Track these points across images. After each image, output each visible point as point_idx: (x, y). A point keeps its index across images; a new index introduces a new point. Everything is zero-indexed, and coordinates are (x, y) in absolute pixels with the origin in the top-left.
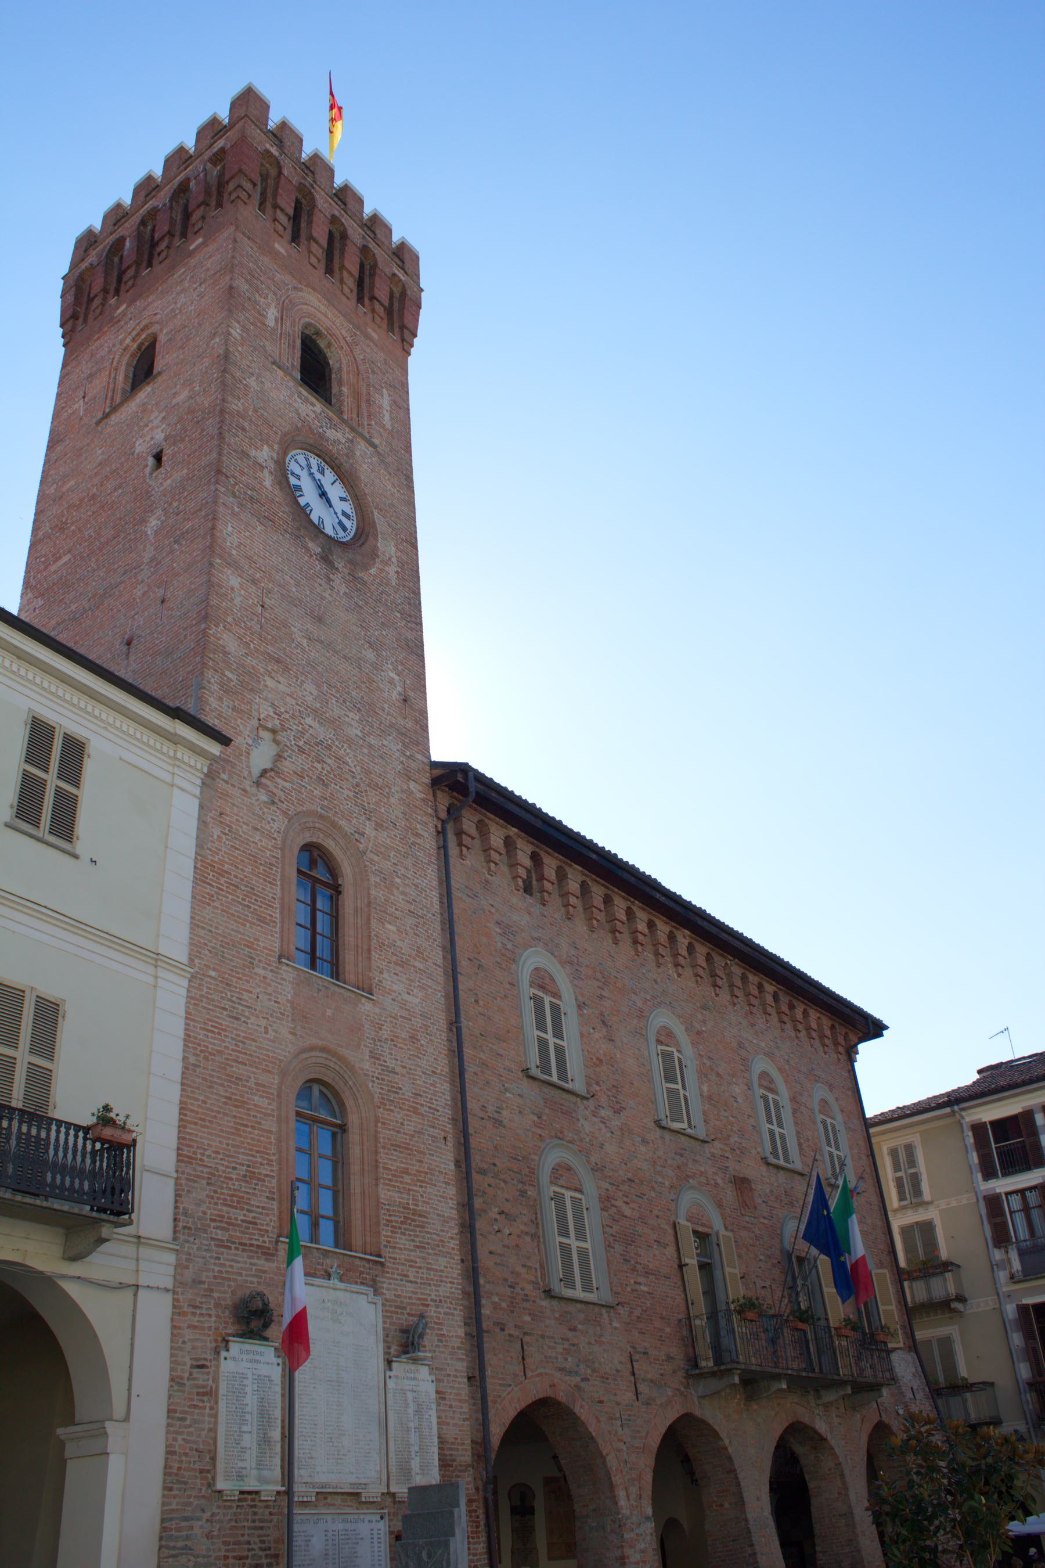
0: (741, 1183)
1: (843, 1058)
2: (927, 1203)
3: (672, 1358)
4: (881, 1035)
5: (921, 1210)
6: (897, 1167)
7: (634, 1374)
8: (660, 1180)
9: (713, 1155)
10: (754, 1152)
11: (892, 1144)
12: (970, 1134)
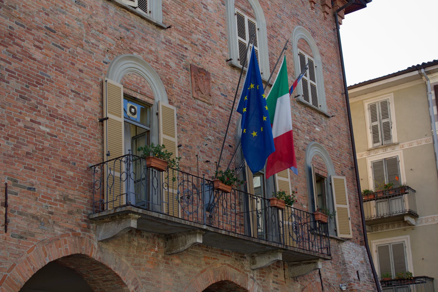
0: (198, 73)
1: (330, 17)
2: (395, 144)
3: (70, 200)
4: (365, 6)
5: (389, 150)
6: (374, 118)
7: (6, 205)
8: (93, 41)
9: (169, 42)
10: (218, 53)
11: (372, 101)
12: (433, 92)
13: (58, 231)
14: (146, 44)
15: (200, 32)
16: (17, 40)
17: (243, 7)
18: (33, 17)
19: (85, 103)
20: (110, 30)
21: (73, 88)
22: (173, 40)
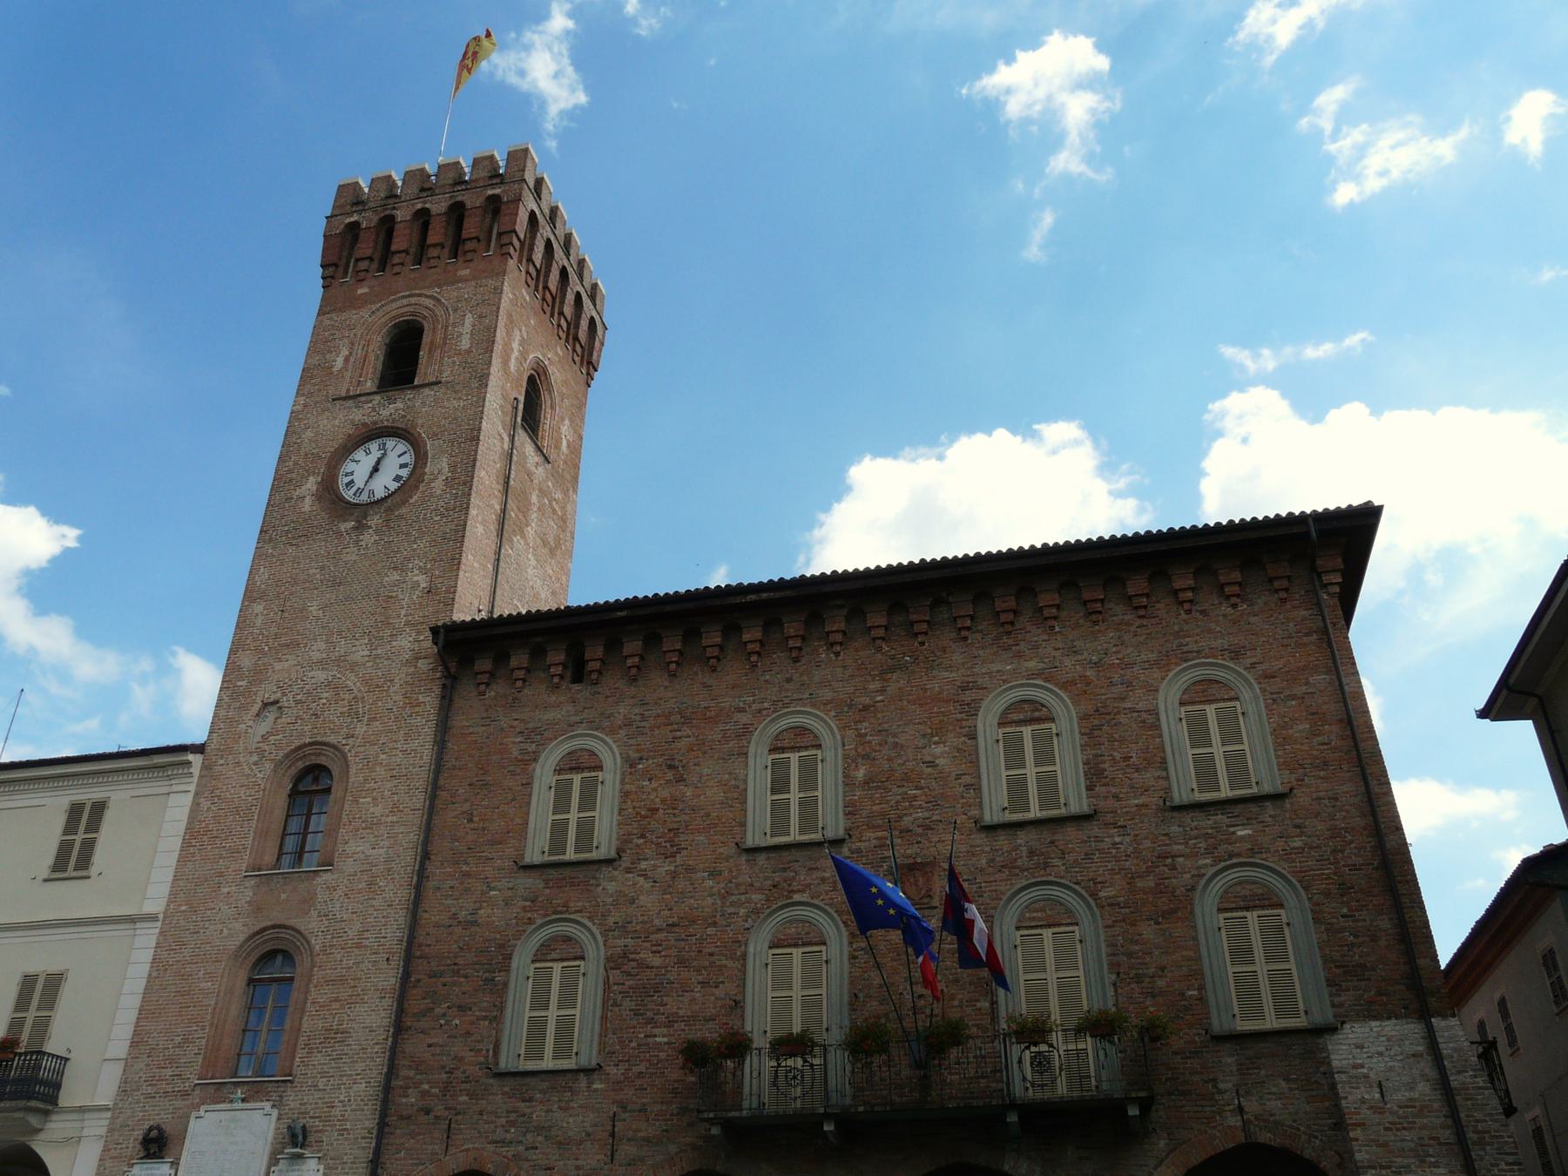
7: (613, 1135)
8: (731, 910)
9: (859, 851)
13: (673, 1149)
15: (920, 807)
19: (717, 992)
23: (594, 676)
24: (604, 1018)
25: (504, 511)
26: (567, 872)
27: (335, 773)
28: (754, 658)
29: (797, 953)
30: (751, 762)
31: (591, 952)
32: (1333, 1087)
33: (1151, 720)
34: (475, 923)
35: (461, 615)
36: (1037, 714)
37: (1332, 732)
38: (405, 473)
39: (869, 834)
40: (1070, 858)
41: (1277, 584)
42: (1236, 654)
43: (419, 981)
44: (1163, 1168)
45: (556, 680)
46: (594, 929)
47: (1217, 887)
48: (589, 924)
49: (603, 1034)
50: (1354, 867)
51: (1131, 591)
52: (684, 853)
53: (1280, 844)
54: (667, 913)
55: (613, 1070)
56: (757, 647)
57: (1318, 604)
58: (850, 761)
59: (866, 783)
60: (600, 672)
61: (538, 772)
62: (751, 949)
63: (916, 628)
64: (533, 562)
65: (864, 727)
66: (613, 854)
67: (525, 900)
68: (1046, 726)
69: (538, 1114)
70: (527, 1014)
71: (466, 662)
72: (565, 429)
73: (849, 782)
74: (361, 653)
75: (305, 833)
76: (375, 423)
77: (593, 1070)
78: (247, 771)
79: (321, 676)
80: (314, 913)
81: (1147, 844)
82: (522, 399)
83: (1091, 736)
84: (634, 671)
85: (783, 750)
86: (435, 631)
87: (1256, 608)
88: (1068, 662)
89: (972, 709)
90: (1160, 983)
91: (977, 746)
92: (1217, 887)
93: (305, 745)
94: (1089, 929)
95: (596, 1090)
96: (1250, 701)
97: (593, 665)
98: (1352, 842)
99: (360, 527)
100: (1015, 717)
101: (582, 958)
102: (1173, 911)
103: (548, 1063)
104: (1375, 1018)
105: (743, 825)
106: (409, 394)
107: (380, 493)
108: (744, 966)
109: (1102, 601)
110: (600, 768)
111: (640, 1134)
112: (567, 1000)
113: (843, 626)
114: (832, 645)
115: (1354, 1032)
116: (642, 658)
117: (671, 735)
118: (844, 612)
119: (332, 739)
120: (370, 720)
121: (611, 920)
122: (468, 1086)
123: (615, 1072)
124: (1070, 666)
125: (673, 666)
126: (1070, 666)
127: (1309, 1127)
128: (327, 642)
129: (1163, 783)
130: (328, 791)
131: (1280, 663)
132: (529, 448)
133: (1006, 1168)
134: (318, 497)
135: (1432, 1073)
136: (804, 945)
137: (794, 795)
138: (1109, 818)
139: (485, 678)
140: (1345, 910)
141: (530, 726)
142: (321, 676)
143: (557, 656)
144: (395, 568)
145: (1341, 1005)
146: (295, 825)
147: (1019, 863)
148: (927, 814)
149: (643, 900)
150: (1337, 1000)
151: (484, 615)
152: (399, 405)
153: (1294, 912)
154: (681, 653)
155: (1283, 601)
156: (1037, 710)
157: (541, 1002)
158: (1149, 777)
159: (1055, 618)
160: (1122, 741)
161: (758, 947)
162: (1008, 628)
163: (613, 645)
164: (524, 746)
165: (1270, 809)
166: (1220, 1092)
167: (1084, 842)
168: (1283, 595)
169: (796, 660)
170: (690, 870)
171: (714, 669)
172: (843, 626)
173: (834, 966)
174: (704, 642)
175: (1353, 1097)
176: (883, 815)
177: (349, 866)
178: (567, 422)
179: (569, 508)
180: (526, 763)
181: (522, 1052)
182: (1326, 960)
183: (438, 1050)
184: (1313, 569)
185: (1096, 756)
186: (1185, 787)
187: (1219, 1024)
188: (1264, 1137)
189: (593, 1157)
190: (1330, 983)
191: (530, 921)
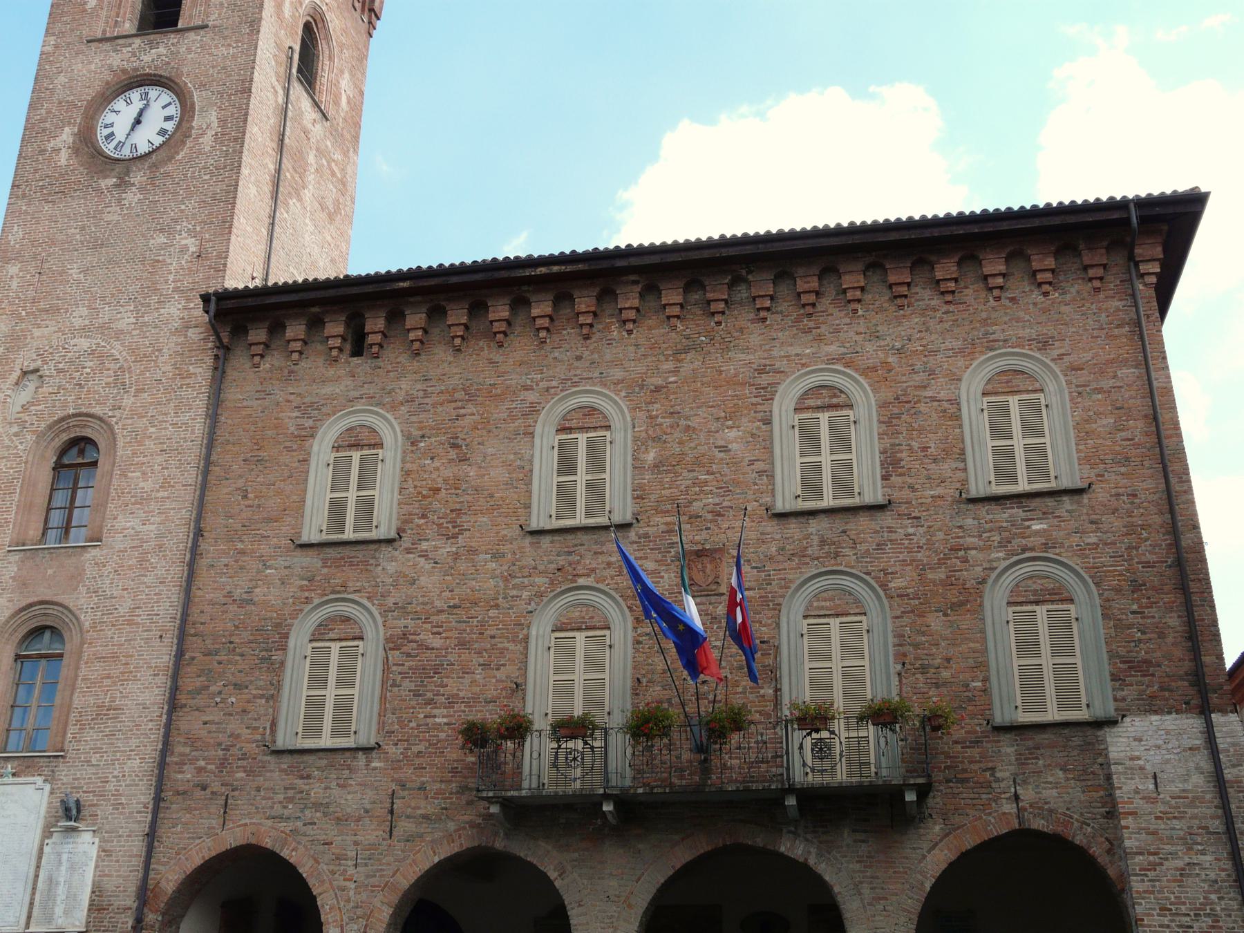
7: (392, 812)
8: (515, 593)
9: (646, 536)
13: (452, 826)
14: (601, 558)
15: (711, 492)
16: (411, 637)
17: (819, 403)
18: (432, 603)
20: (541, 568)
21: (481, 660)
22: (650, 530)
23: (375, 349)
24: (383, 698)
25: (279, 171)
26: (347, 551)
27: (102, 445)
28: (543, 334)
29: (580, 637)
30: (537, 441)
31: (369, 632)
32: (1109, 778)
33: (952, 409)
34: (251, 601)
35: (235, 281)
36: (835, 401)
37: (1138, 428)
38: (170, 126)
39: (658, 519)
40: (862, 548)
41: (1091, 273)
42: (1044, 344)
43: (193, 658)
44: (936, 851)
45: (335, 353)
46: (373, 609)
47: (1009, 580)
48: (368, 605)
49: (382, 714)
50: (1147, 565)
51: (939, 275)
52: (467, 534)
53: (1075, 539)
54: (447, 594)
55: (391, 749)
56: (545, 322)
57: (1133, 295)
58: (640, 443)
59: (656, 466)
60: (381, 346)
61: (315, 448)
62: (533, 632)
63: (713, 307)
64: (311, 228)
65: (656, 408)
66: (393, 534)
67: (303, 579)
68: (844, 413)
69: (316, 791)
70: (305, 693)
71: (239, 330)
72: (345, 83)
73: (638, 466)
74: (126, 320)
75: (71, 507)
76: (136, 69)
77: (372, 749)
78: (7, 442)
79: (84, 343)
80: (83, 590)
81: (940, 535)
82: (297, 48)
83: (889, 423)
84: (417, 345)
85: (570, 430)
86: (206, 298)
87: (1068, 297)
88: (870, 347)
89: (767, 394)
90: (946, 674)
91: (771, 431)
92: (1009, 580)
93: (69, 417)
94: (878, 620)
95: (375, 769)
96: (1055, 394)
97: (371, 339)
98: (1147, 540)
99: (123, 184)
100: (811, 403)
101: (362, 638)
102: (962, 604)
103: (326, 741)
104: (1156, 712)
105: (528, 507)
106: (173, 38)
107: (143, 148)
108: (526, 648)
109: (909, 284)
110: (379, 445)
111: (419, 812)
112: (346, 679)
113: (636, 303)
114: (624, 322)
115: (1134, 725)
116: (426, 331)
117: (454, 413)
118: (638, 288)
119: (98, 410)
120: (138, 391)
121: (390, 601)
122: (245, 763)
123: (393, 751)
124: (871, 352)
125: (458, 341)
126: (871, 352)
127: (1082, 814)
128: (89, 307)
129: (960, 475)
130: (94, 464)
131: (1087, 356)
132: (306, 103)
133: (782, 849)
134: (76, 151)
135: (1207, 766)
136: (588, 628)
137: (581, 477)
138: (903, 509)
139: (259, 349)
140: (1135, 607)
141: (307, 400)
142: (84, 343)
143: (335, 328)
144: (162, 230)
145: (1124, 699)
146: (61, 498)
147: (810, 552)
148: (717, 500)
149: (423, 580)
150: (1119, 694)
151: (258, 283)
152: (162, 50)
153: (1085, 608)
154: (466, 327)
155: (1097, 290)
156: (835, 396)
157: (318, 680)
158: (946, 468)
159: (859, 301)
160: (921, 430)
161: (541, 630)
162: (809, 309)
163: (395, 317)
164: (299, 421)
165: (1067, 503)
166: (998, 780)
167: (876, 532)
168: (1097, 284)
169: (587, 337)
170: (472, 551)
171: (501, 345)
172: (636, 303)
173: (618, 651)
174: (491, 316)
175: (1126, 788)
176: (672, 500)
177: (118, 542)
178: (347, 75)
179: (349, 169)
180: (303, 438)
181: (300, 730)
182: (1112, 655)
183: (213, 728)
184: (1131, 257)
185: (893, 445)
186: (983, 480)
187: (1001, 716)
188: (1038, 824)
189: (371, 833)
190: (1114, 678)
191: (308, 600)
